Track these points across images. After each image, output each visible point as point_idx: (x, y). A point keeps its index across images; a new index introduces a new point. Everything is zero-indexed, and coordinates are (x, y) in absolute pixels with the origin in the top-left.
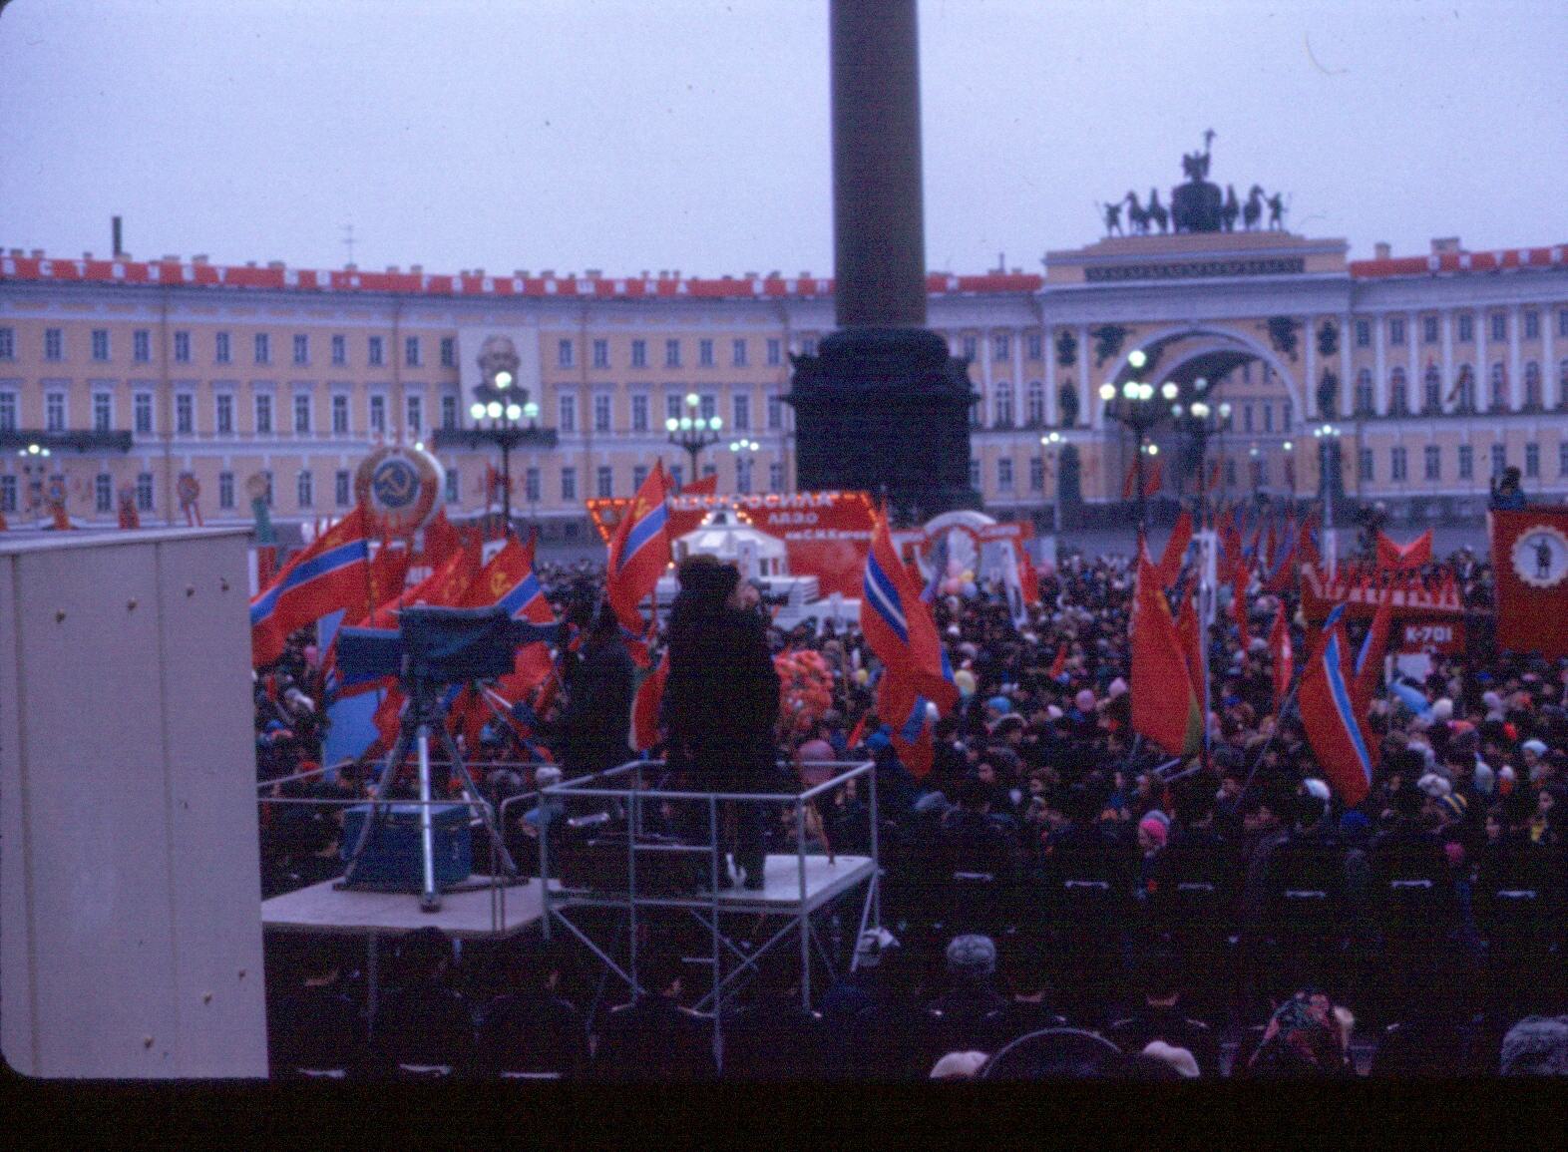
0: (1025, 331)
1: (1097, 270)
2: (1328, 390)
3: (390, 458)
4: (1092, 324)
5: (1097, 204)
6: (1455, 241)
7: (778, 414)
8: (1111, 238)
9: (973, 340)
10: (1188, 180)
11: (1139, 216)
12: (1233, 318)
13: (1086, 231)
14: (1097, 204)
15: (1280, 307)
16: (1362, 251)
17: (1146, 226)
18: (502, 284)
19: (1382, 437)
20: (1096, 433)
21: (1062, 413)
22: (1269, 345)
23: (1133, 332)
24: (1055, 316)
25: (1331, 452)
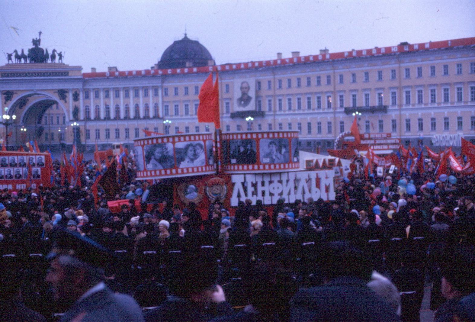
1: (5, 74)
2: (76, 112)
4: (3, 91)
5: (4, 53)
8: (8, 64)
10: (34, 47)
11: (18, 57)
12: (47, 90)
14: (4, 53)
15: (62, 86)
16: (86, 70)
17: (20, 61)
19: (92, 126)
23: (16, 93)
25: (77, 130)
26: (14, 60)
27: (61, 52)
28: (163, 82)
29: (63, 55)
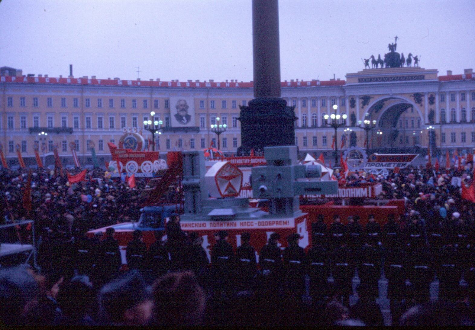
0: (340, 98)
1: (362, 79)
2: (432, 115)
3: (129, 136)
4: (360, 95)
5: (362, 59)
7: (236, 123)
8: (366, 69)
9: (325, 100)
10: (390, 51)
11: (375, 62)
12: (403, 94)
13: (358, 67)
16: (442, 73)
17: (377, 66)
18: (183, 84)
19: (448, 129)
21: (351, 123)
23: (373, 98)
24: (348, 93)
25: (433, 133)
26: (371, 66)
29: (419, 59)
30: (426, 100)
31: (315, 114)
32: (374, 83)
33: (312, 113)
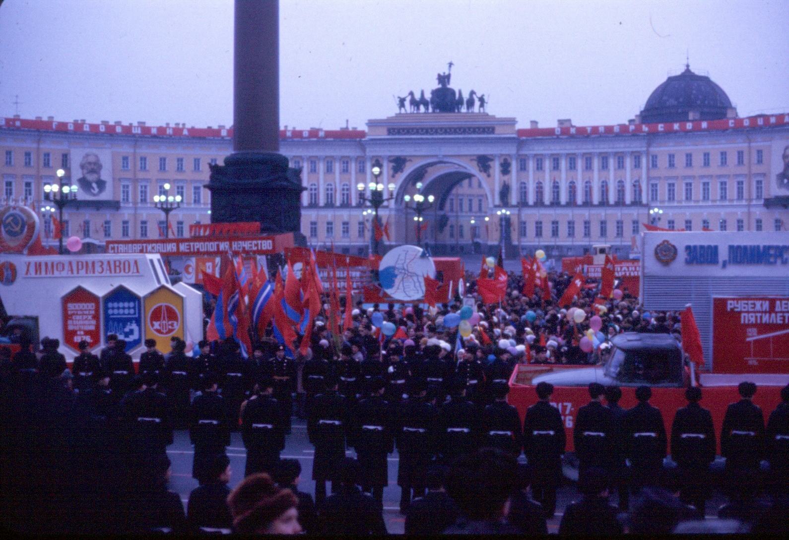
0: (357, 159)
1: (394, 129)
2: (505, 192)
4: (390, 156)
5: (394, 96)
6: (569, 120)
8: (400, 113)
9: (331, 162)
10: (440, 86)
11: (415, 103)
12: (460, 156)
13: (389, 110)
14: (394, 96)
15: (482, 150)
16: (523, 124)
17: (418, 109)
18: (94, 127)
19: (531, 215)
20: (391, 210)
22: (477, 169)
23: (410, 160)
24: (371, 152)
25: (506, 222)
26: (408, 108)
27: (483, 95)
28: (649, 145)
30: (496, 167)
31: (347, 185)
32: (470, 136)
33: (342, 184)
